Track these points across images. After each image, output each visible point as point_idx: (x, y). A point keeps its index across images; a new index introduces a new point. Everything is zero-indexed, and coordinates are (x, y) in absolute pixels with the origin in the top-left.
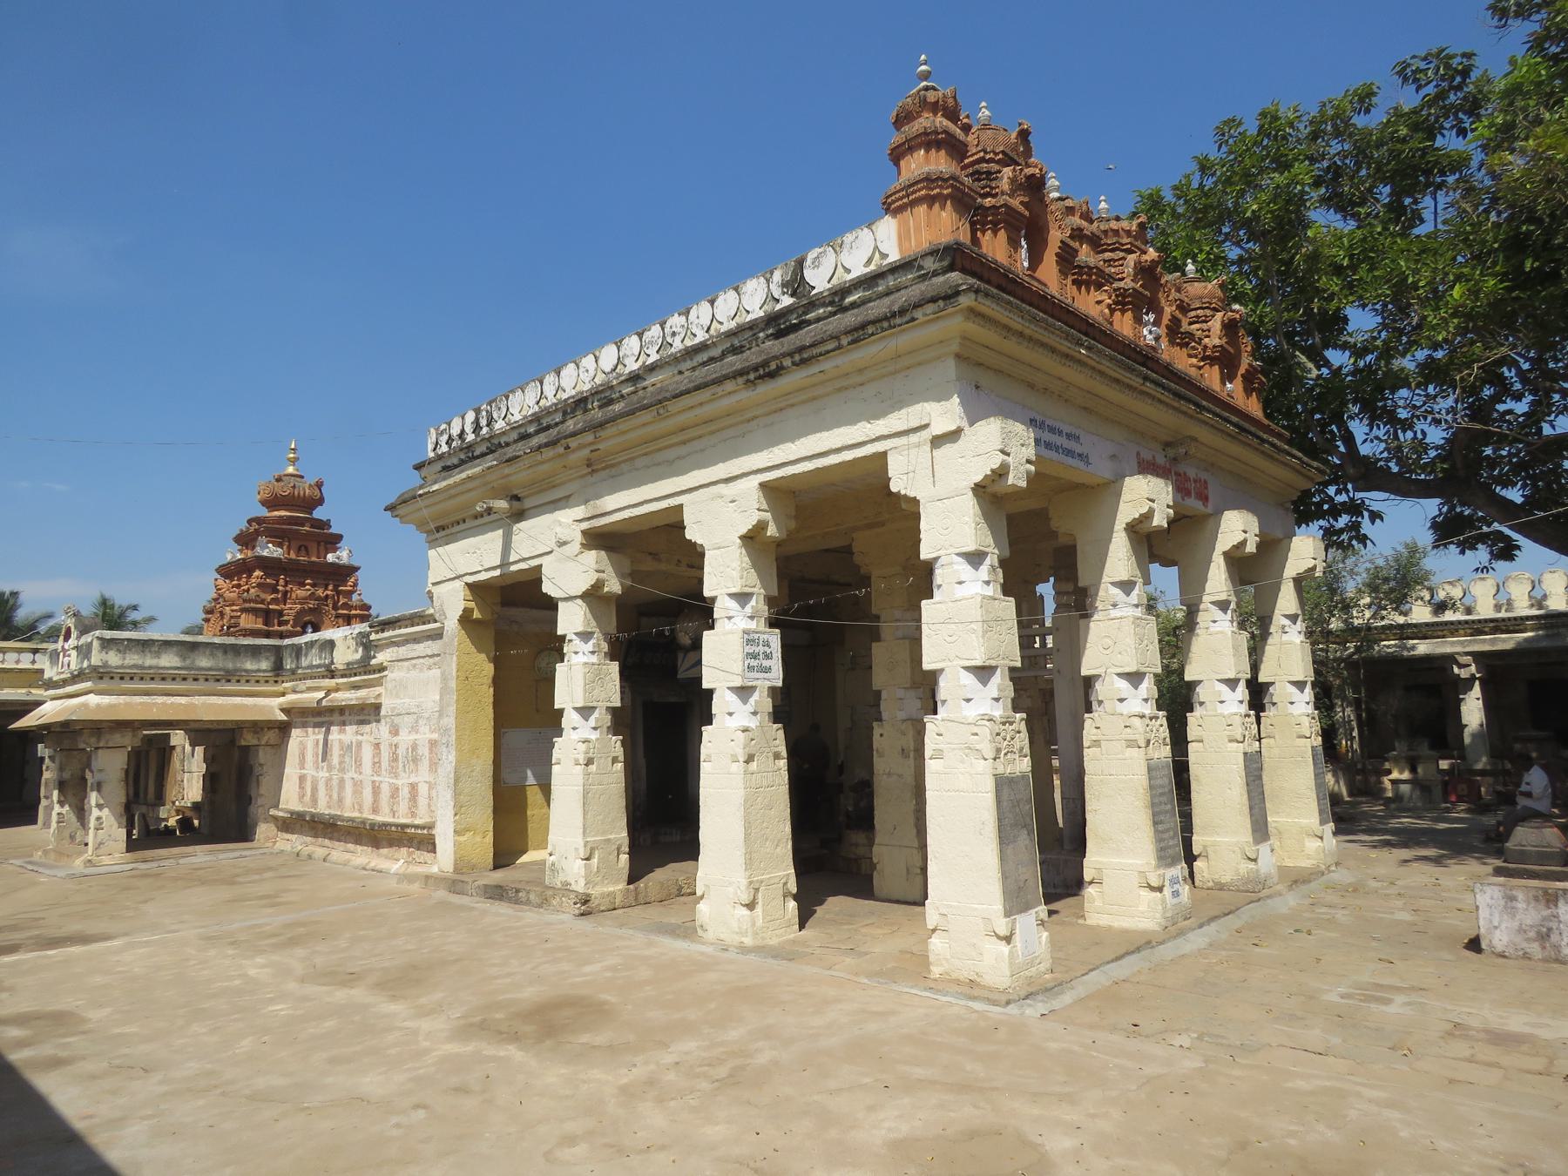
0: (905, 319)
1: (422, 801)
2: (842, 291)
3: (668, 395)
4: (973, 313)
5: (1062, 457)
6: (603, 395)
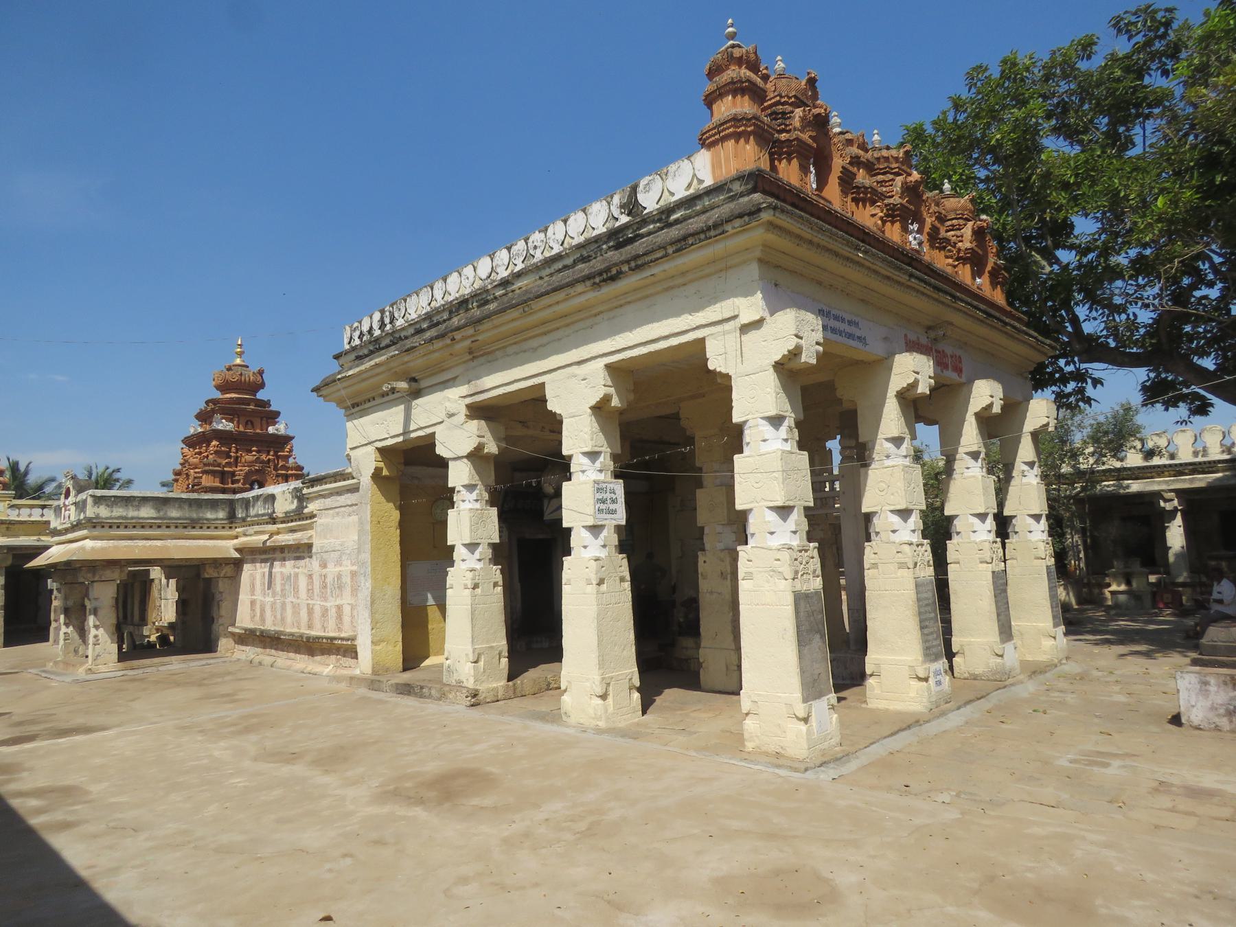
0: (717, 232)
1: (346, 619)
2: (668, 211)
3: (531, 296)
4: (771, 226)
6: (480, 297)
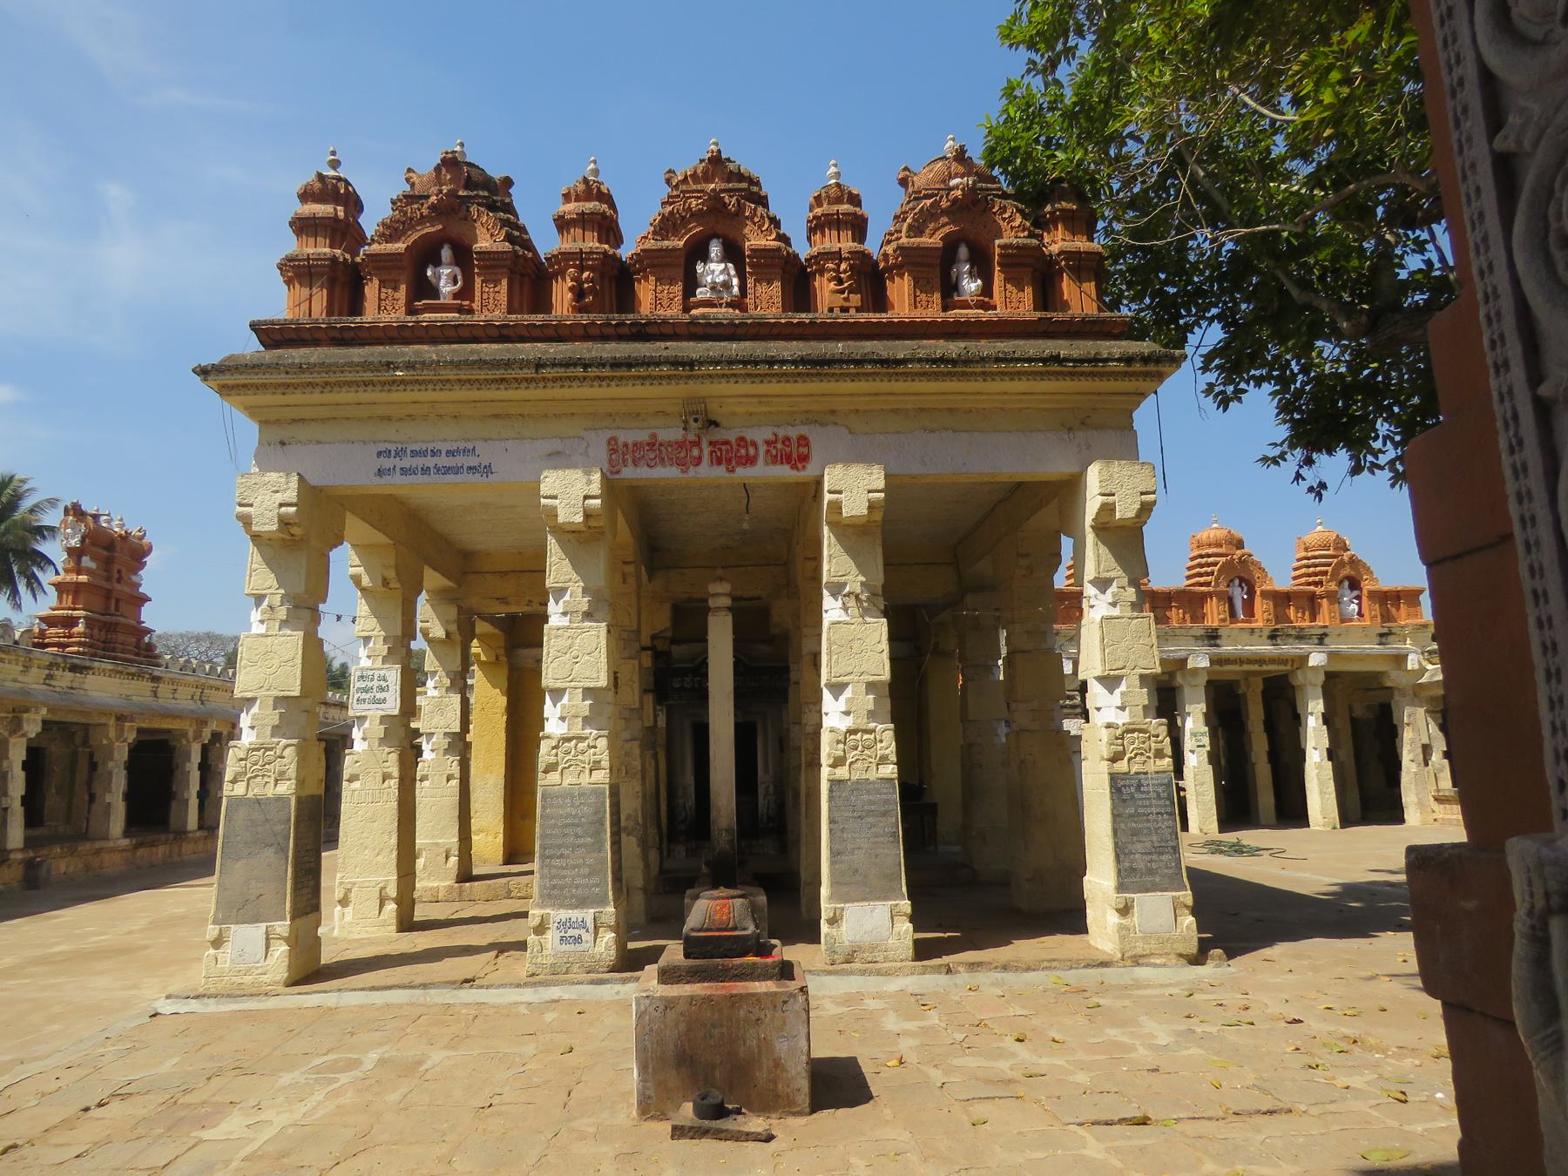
5: (434, 478)
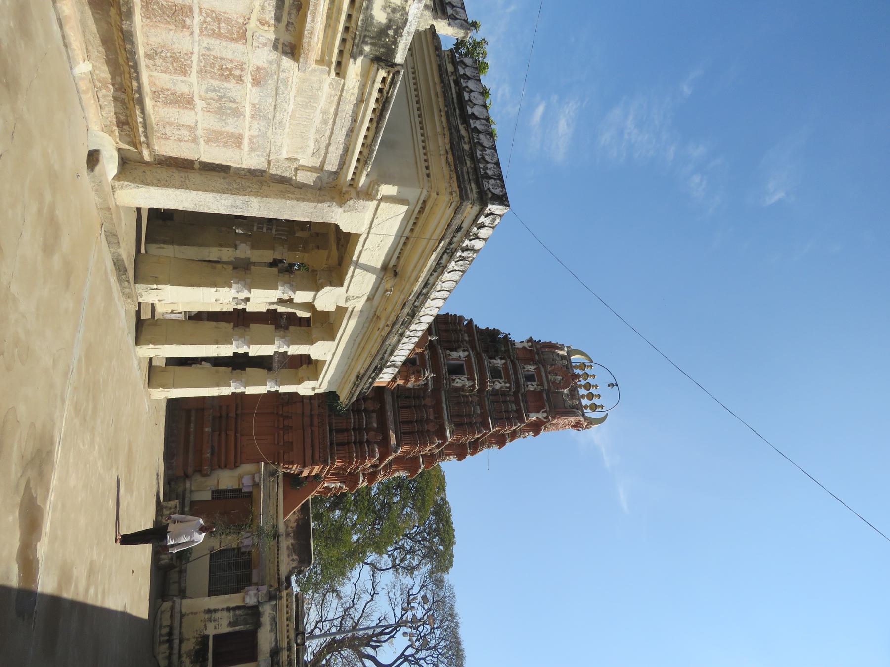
1: (172, 113)
